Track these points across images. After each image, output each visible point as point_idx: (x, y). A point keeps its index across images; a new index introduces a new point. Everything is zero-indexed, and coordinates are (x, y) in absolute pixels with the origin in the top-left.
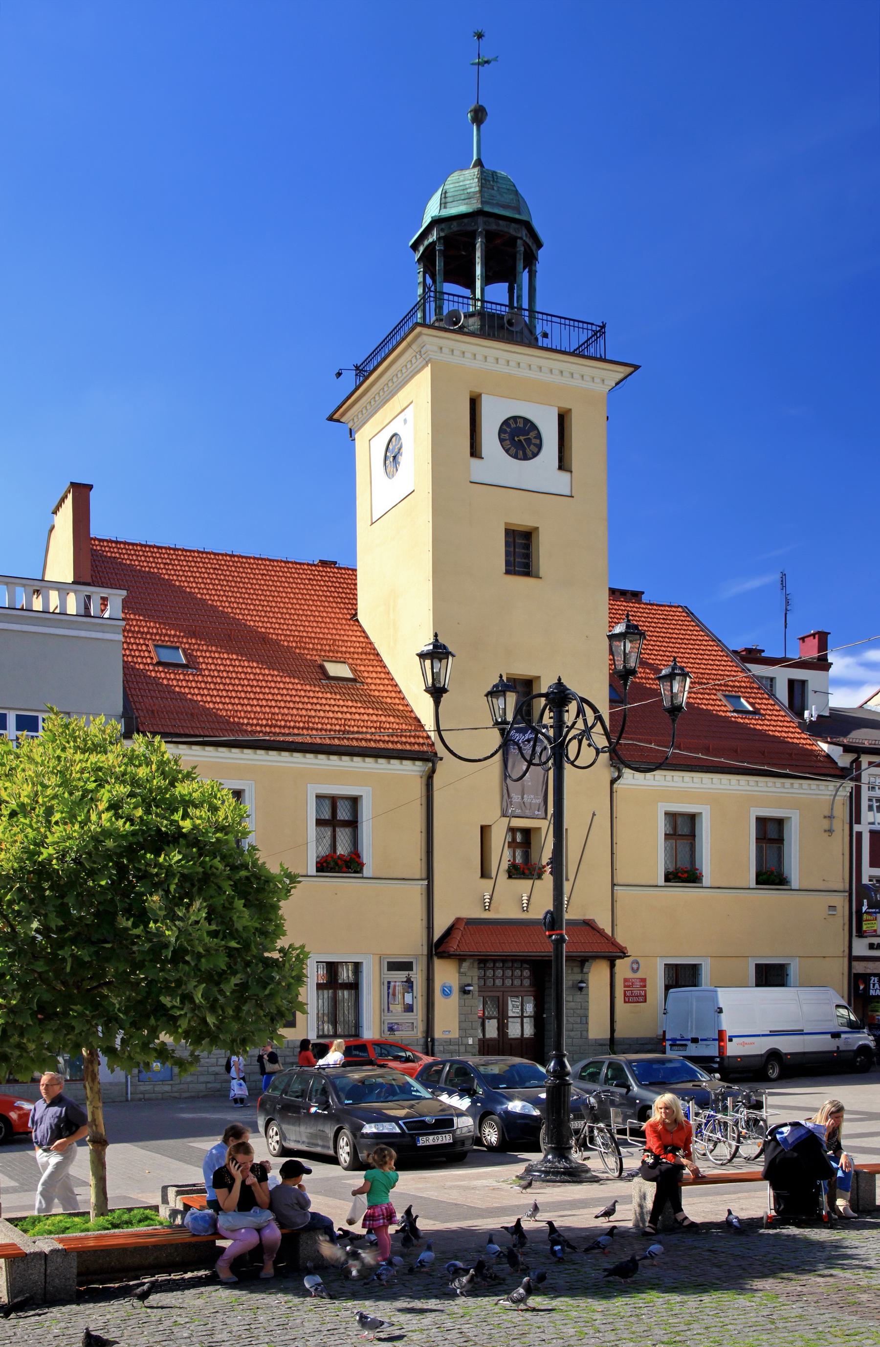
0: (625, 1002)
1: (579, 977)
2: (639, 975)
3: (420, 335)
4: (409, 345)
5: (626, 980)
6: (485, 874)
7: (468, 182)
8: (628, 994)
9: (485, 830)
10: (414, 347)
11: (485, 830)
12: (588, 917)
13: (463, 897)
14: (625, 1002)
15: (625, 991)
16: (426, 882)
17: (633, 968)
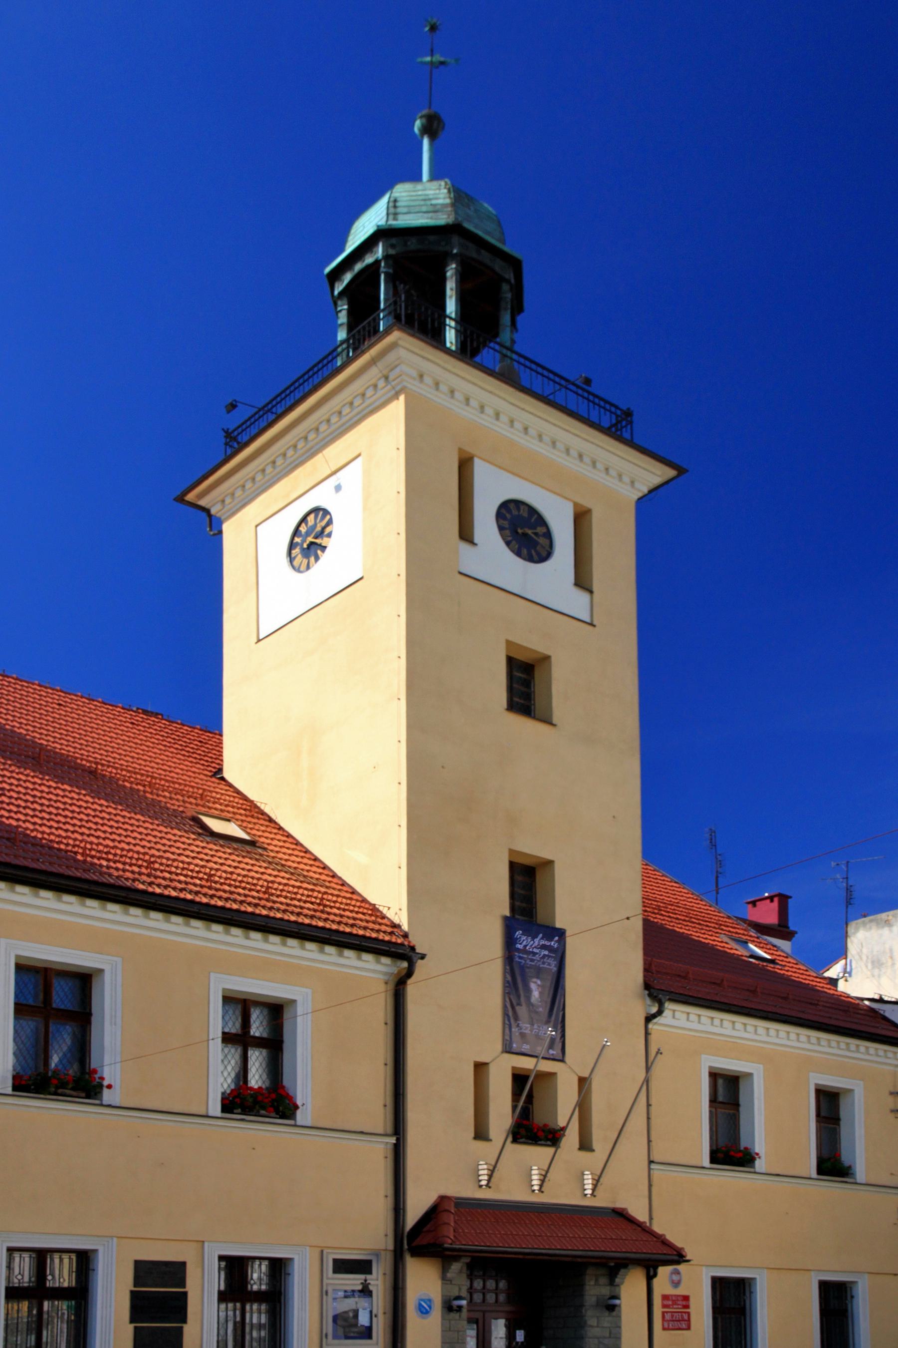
0: (664, 1329)
1: (605, 1291)
2: (681, 1291)
3: (393, 346)
4: (373, 362)
5: (665, 1297)
6: (481, 1134)
7: (432, 192)
8: (668, 1317)
9: (480, 1068)
10: (381, 364)
11: (480, 1068)
12: (619, 1205)
13: (455, 1163)
14: (664, 1329)
15: (663, 1313)
16: (393, 1140)
17: (673, 1282)
